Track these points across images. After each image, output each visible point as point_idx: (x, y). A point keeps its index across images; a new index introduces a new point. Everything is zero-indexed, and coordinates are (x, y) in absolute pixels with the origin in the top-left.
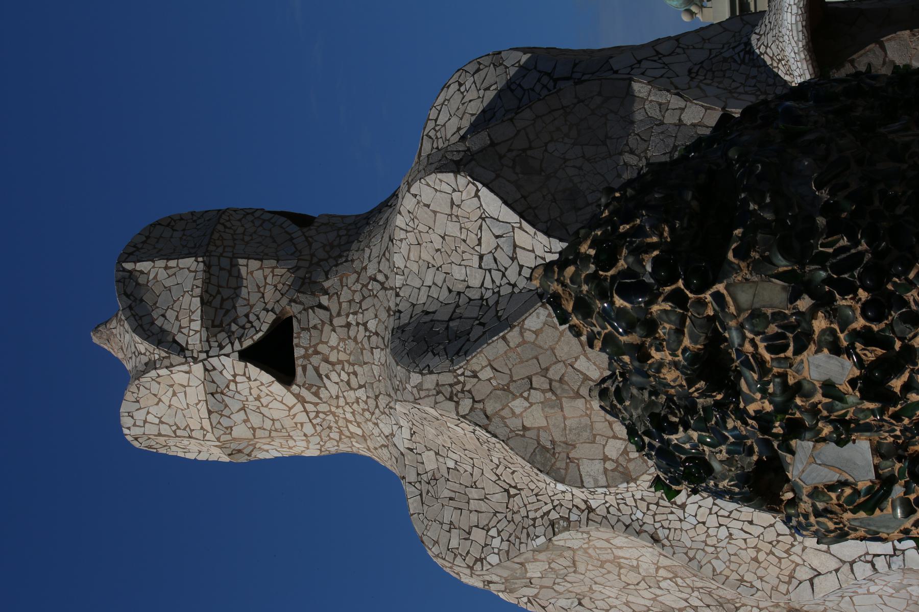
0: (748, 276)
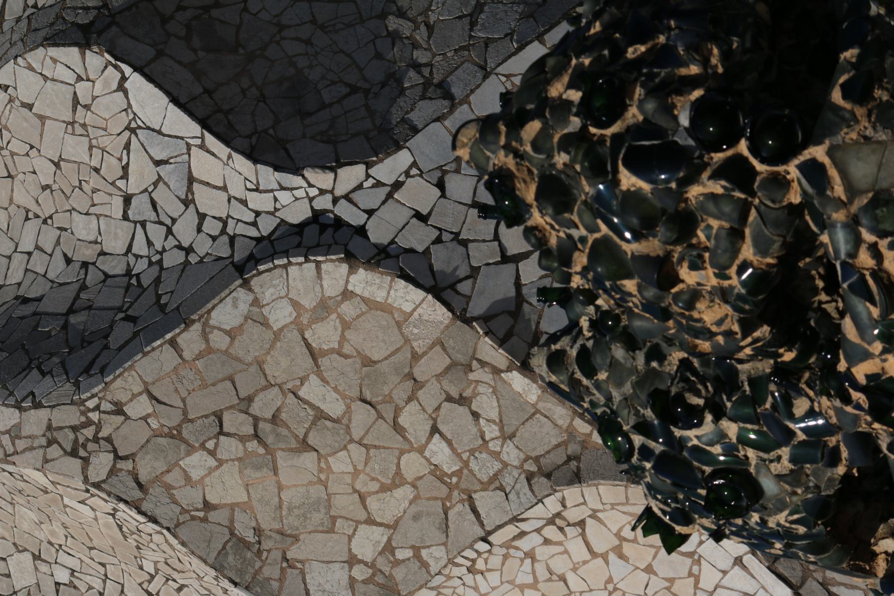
0: (869, 132)
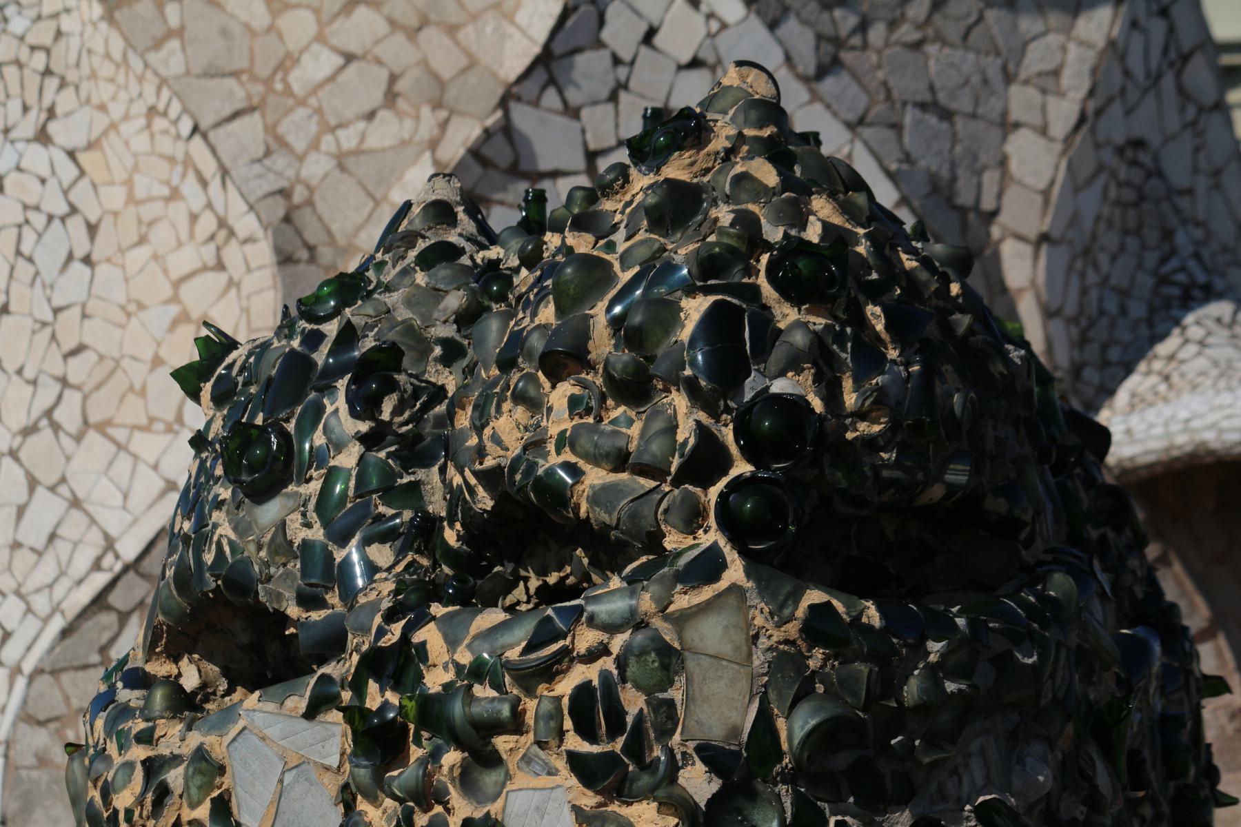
0: (763, 642)
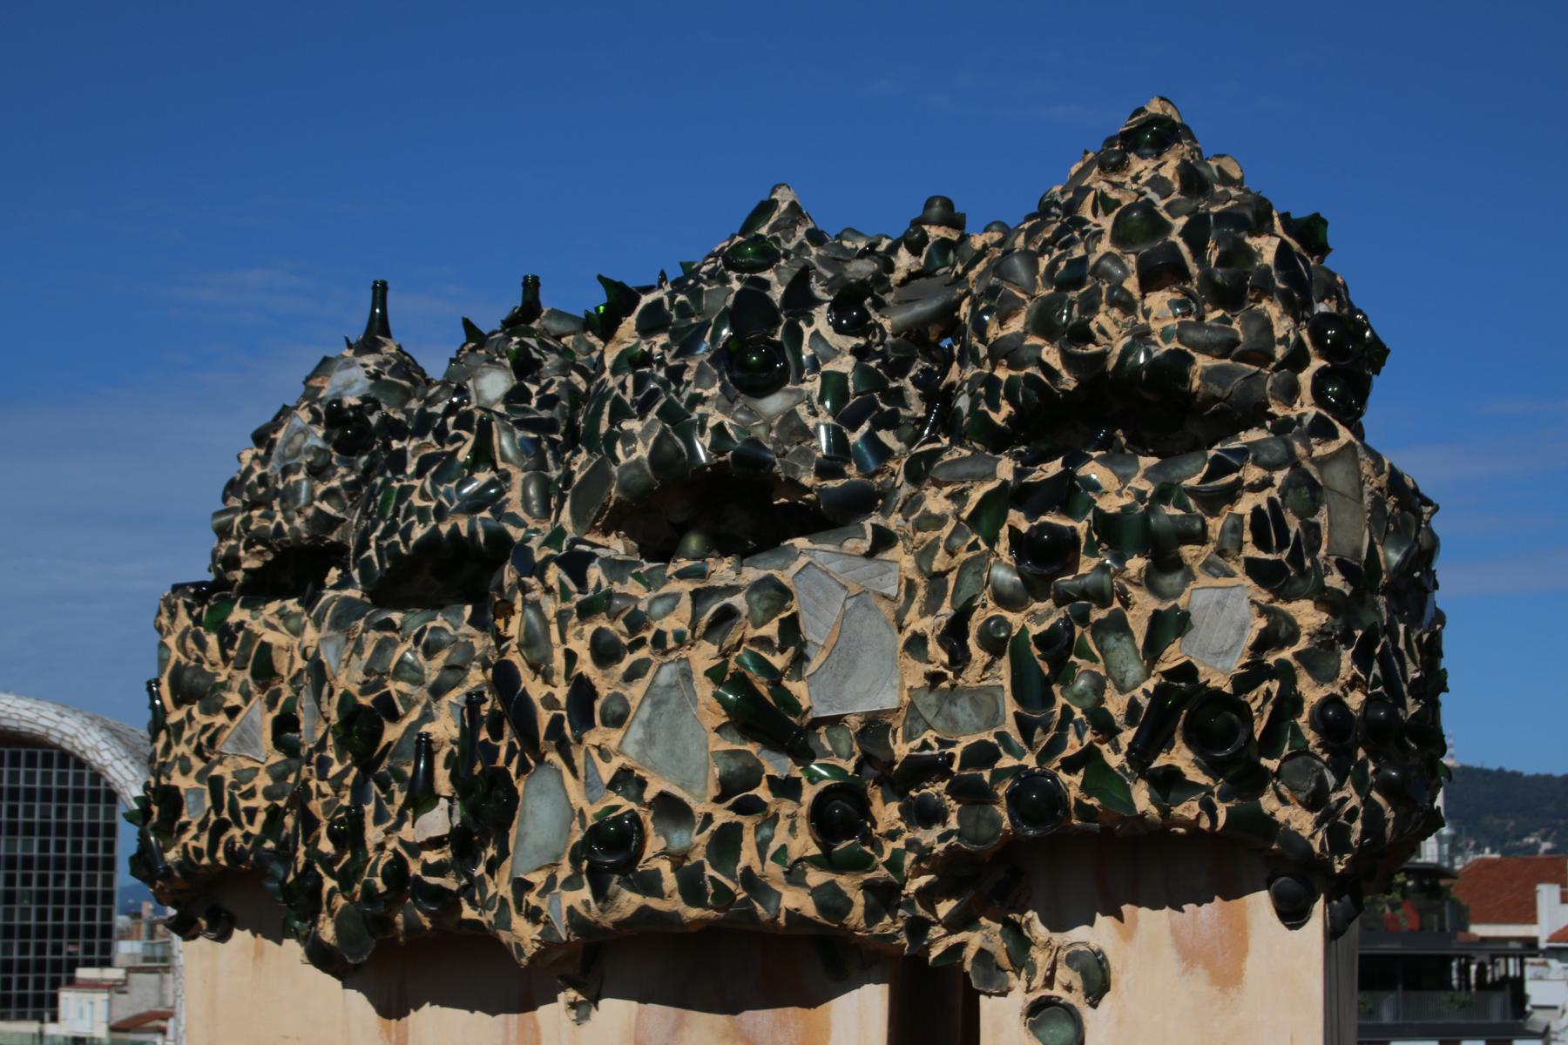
0: (1367, 488)
